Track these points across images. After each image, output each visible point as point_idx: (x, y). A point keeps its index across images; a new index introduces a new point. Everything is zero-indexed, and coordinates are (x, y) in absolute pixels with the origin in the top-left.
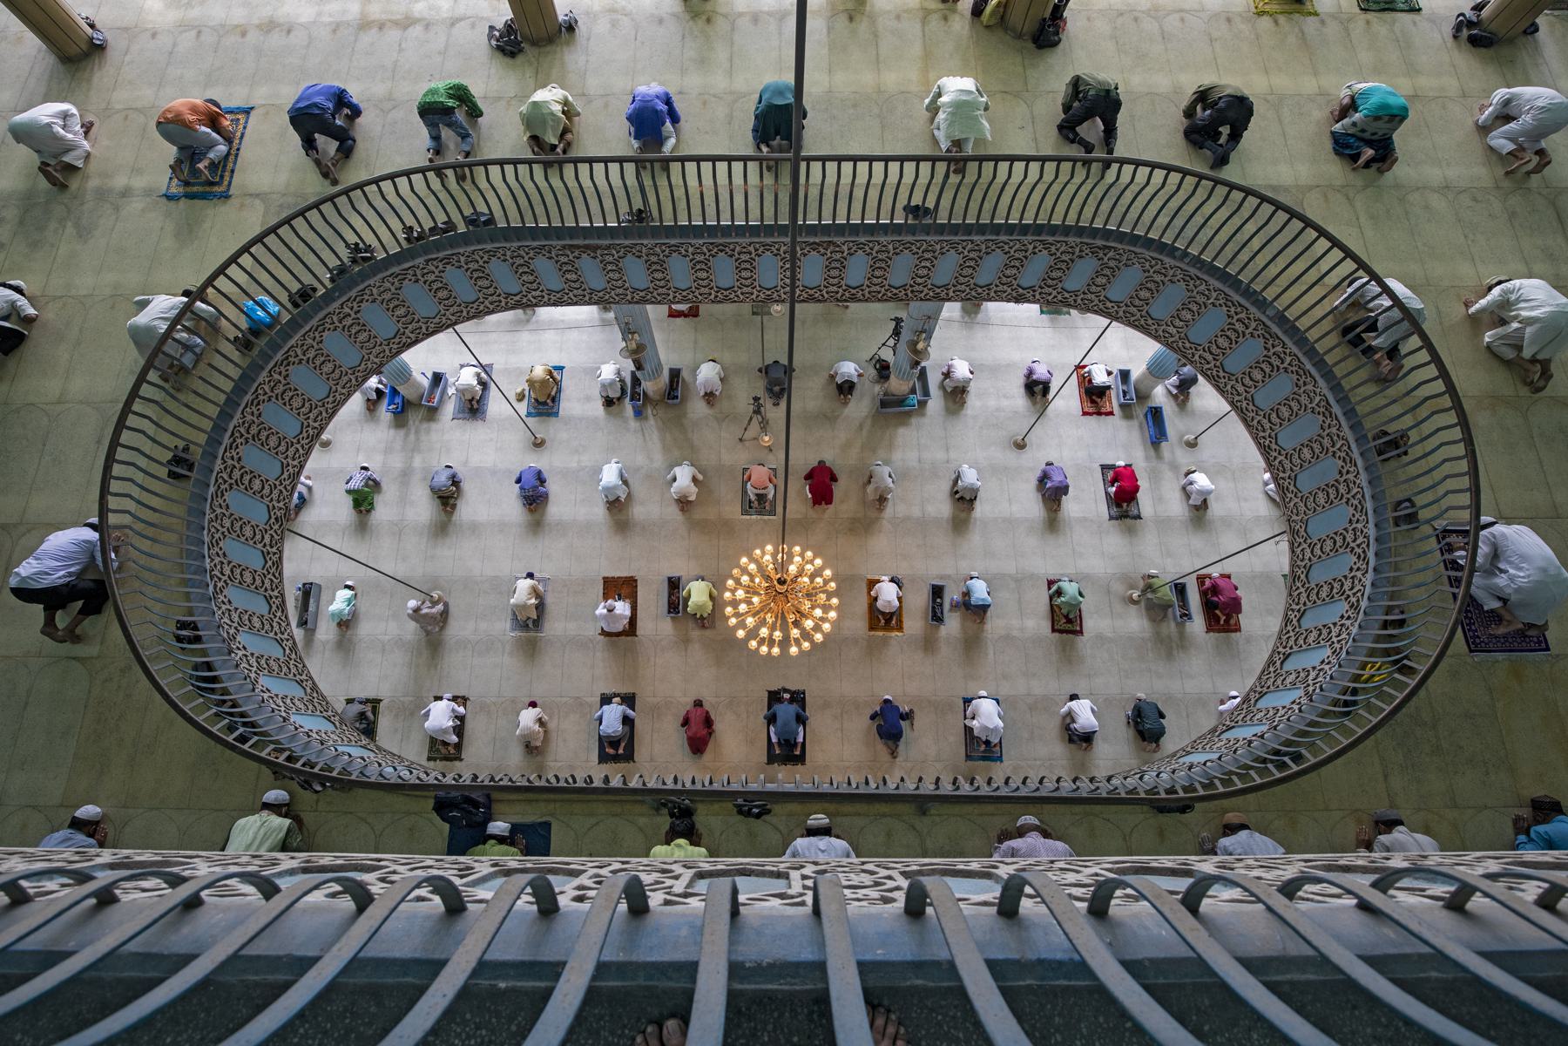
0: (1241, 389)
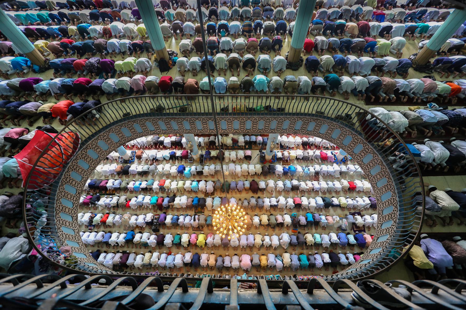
0: (359, 158)
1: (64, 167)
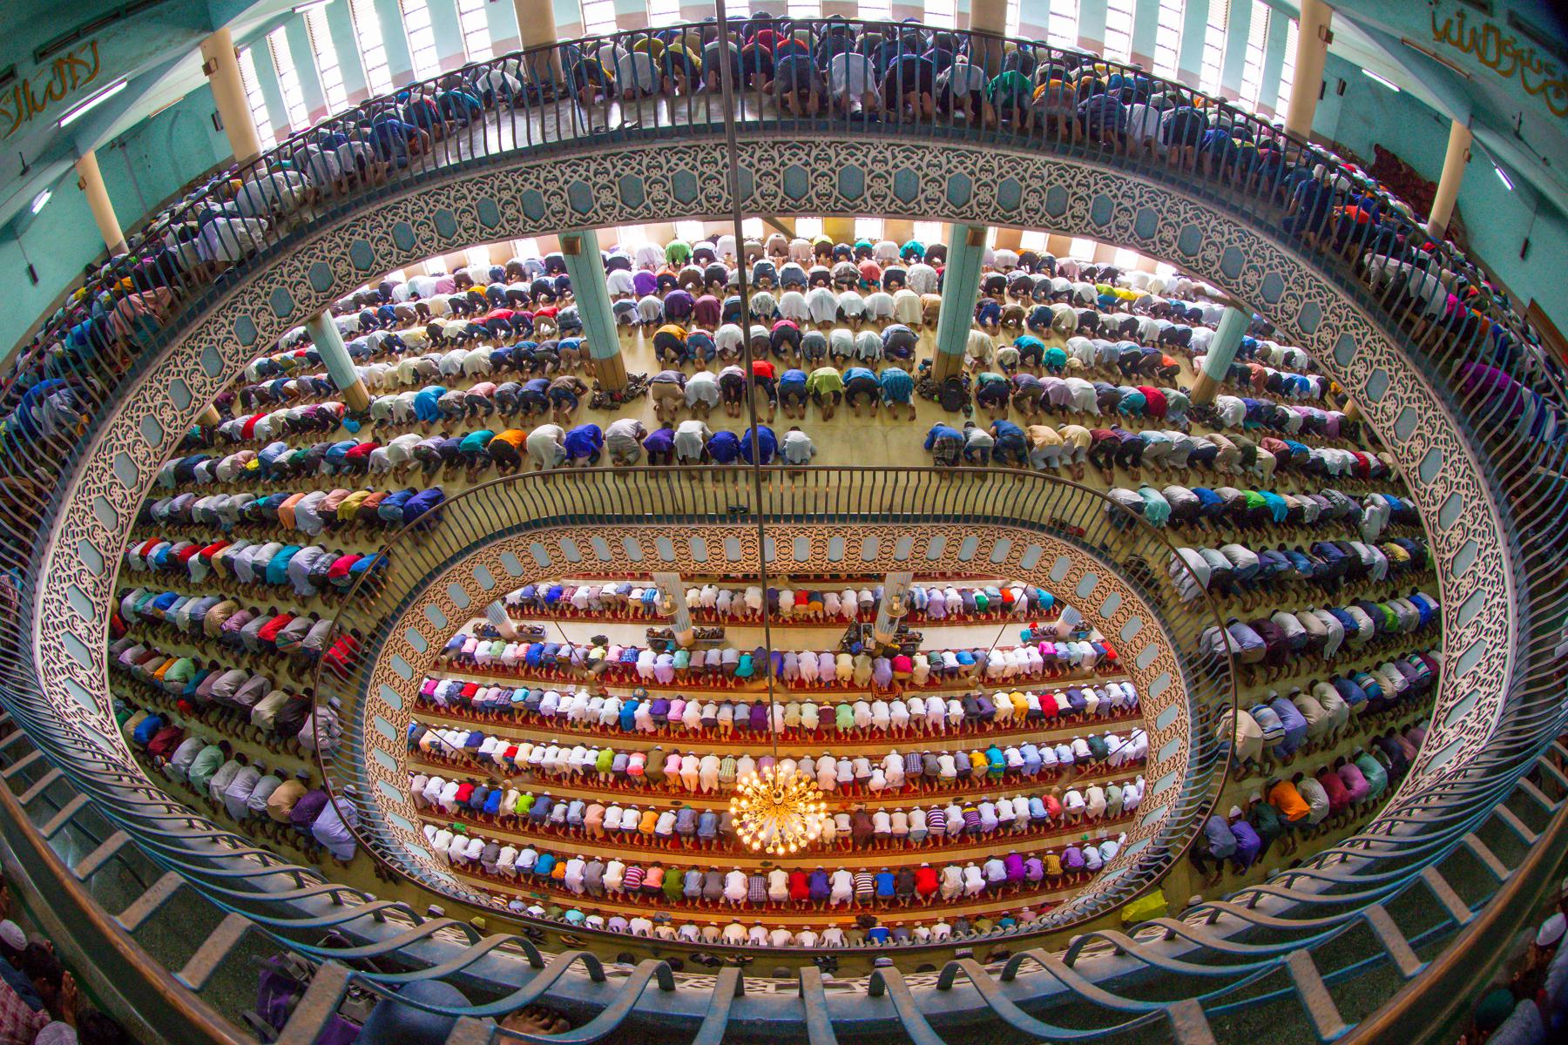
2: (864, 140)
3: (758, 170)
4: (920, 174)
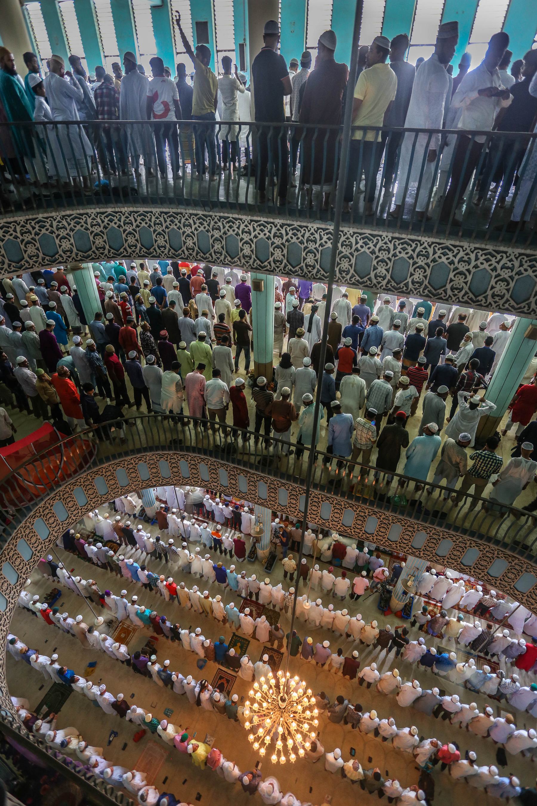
1: (52, 489)
2: (457, 243)
3: (377, 257)
4: (494, 274)
